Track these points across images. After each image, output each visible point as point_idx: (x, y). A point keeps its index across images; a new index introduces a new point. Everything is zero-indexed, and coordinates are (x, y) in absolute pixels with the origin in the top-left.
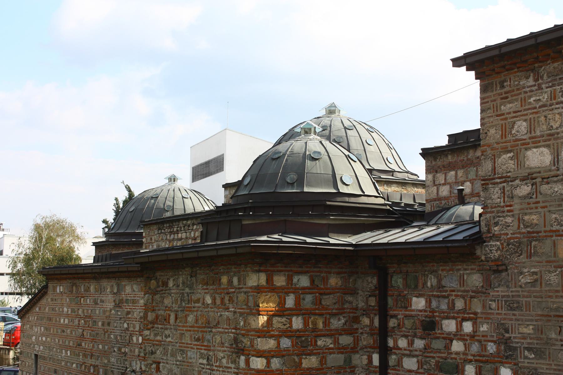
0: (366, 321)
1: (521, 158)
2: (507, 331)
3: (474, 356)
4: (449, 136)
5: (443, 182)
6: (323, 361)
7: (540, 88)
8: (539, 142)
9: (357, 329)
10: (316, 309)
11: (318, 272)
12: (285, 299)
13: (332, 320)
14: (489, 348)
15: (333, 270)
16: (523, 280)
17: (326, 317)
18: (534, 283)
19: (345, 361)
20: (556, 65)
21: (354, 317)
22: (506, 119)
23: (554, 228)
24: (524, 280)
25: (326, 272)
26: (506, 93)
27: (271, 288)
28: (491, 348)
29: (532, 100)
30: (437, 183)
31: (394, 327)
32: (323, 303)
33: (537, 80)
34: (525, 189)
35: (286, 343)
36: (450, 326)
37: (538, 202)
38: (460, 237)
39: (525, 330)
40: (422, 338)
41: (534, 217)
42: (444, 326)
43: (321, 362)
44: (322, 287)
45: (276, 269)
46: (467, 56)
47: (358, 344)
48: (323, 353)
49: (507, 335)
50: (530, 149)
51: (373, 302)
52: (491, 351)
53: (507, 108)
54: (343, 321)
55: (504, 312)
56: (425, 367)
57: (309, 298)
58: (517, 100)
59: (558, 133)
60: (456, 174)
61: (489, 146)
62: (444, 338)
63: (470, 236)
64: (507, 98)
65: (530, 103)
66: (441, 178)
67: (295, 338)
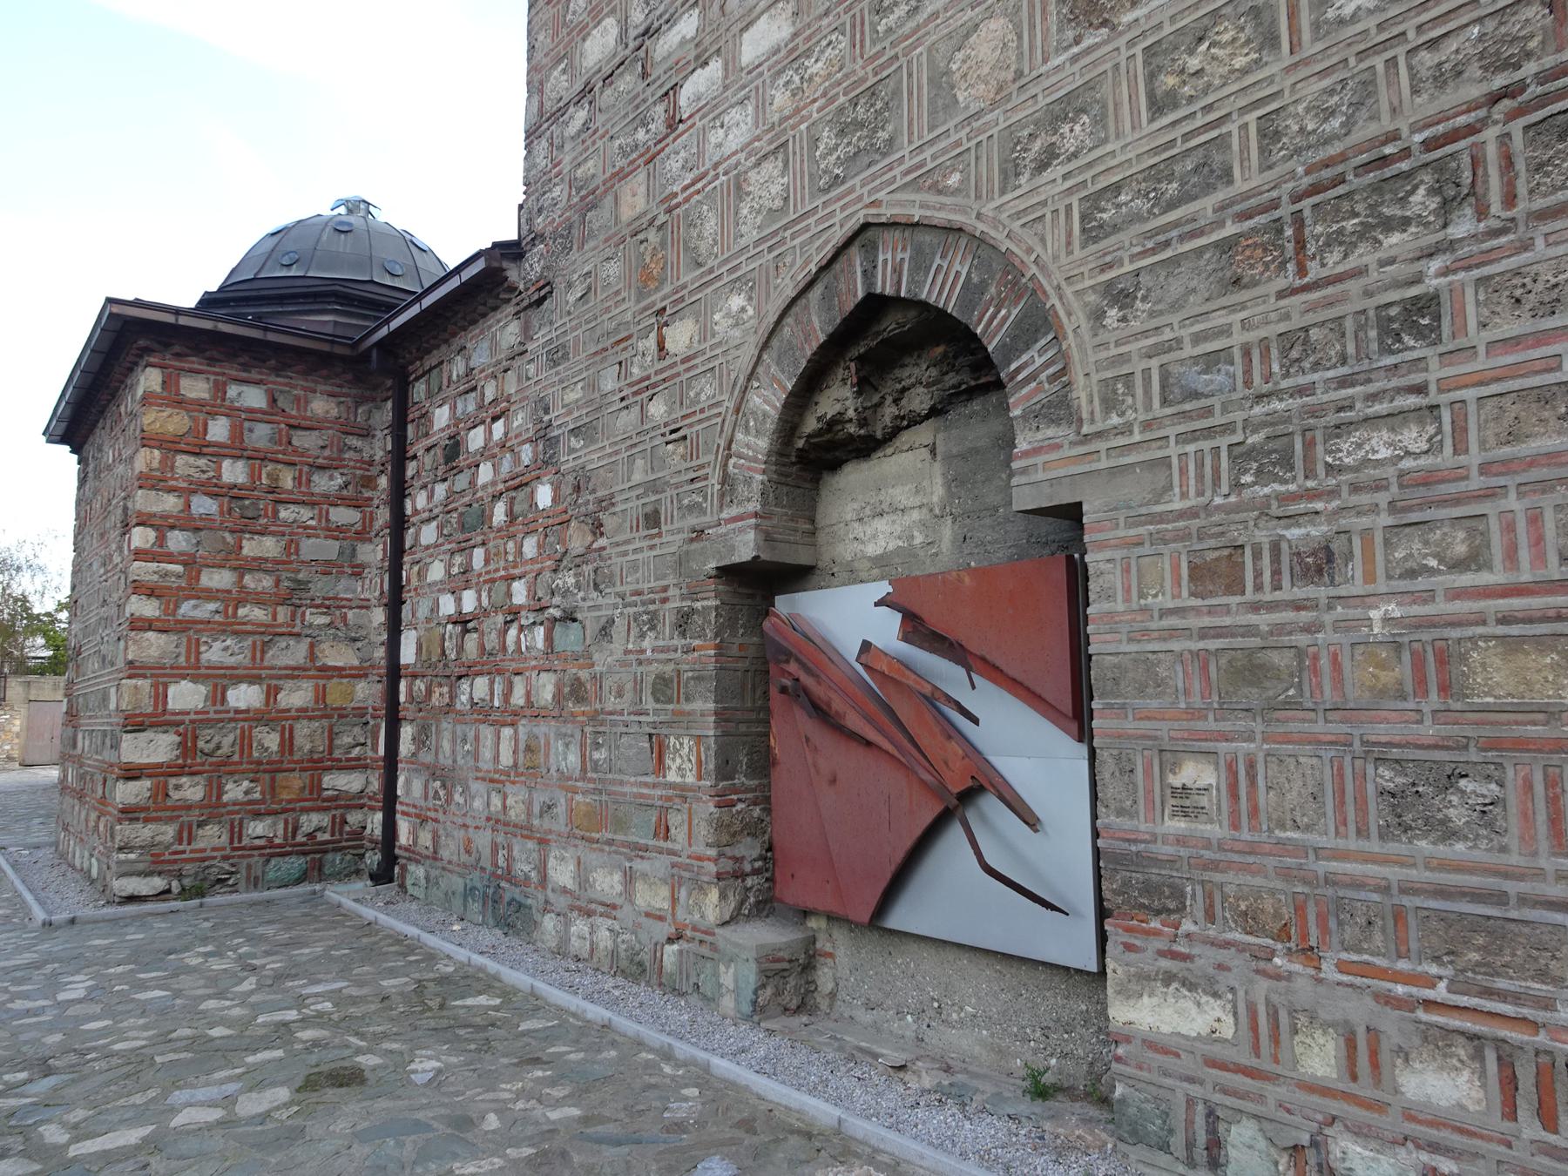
6: (292, 547)
9: (371, 499)
10: (278, 452)
11: (286, 385)
12: (206, 425)
13: (315, 478)
15: (320, 387)
17: (301, 471)
19: (340, 554)
21: (363, 477)
25: (304, 389)
32: (295, 442)
35: (204, 505)
43: (287, 548)
44: (294, 413)
45: (186, 366)
47: (371, 526)
54: (340, 481)
67: (226, 500)
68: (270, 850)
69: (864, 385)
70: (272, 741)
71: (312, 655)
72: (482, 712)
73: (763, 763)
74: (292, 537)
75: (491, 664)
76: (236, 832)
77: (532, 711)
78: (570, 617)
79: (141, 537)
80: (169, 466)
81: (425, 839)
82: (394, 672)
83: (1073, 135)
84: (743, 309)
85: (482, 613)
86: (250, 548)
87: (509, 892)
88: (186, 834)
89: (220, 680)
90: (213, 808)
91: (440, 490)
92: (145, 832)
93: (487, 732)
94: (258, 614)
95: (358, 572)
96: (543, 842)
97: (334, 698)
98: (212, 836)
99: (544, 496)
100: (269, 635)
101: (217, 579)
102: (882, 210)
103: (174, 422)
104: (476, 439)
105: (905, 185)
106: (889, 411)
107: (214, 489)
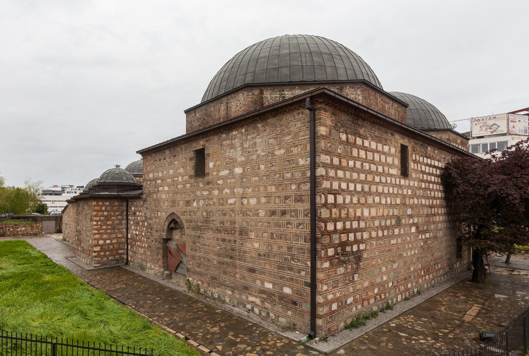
6: (113, 222)
24: (149, 203)
27: (98, 205)
34: (149, 183)
35: (102, 218)
48: (113, 221)
53: (147, 164)
57: (109, 208)
68: (112, 260)
69: (175, 224)
70: (112, 247)
71: (116, 236)
72: (139, 246)
73: (167, 257)
74: (113, 221)
75: (140, 241)
76: (108, 258)
77: (144, 247)
78: (149, 238)
79: (95, 223)
80: (98, 213)
81: (132, 259)
82: (127, 238)
83: (186, 214)
85: (139, 235)
86: (108, 223)
87: (143, 267)
88: (102, 259)
89: (105, 240)
90: (105, 256)
92: (97, 259)
93: (140, 249)
94: (109, 231)
95: (122, 224)
96: (146, 262)
97: (119, 240)
98: (105, 259)
99: (146, 224)
100: (111, 234)
101: (104, 227)
103: (98, 208)
104: (138, 213)
106: (177, 227)
107: (103, 216)
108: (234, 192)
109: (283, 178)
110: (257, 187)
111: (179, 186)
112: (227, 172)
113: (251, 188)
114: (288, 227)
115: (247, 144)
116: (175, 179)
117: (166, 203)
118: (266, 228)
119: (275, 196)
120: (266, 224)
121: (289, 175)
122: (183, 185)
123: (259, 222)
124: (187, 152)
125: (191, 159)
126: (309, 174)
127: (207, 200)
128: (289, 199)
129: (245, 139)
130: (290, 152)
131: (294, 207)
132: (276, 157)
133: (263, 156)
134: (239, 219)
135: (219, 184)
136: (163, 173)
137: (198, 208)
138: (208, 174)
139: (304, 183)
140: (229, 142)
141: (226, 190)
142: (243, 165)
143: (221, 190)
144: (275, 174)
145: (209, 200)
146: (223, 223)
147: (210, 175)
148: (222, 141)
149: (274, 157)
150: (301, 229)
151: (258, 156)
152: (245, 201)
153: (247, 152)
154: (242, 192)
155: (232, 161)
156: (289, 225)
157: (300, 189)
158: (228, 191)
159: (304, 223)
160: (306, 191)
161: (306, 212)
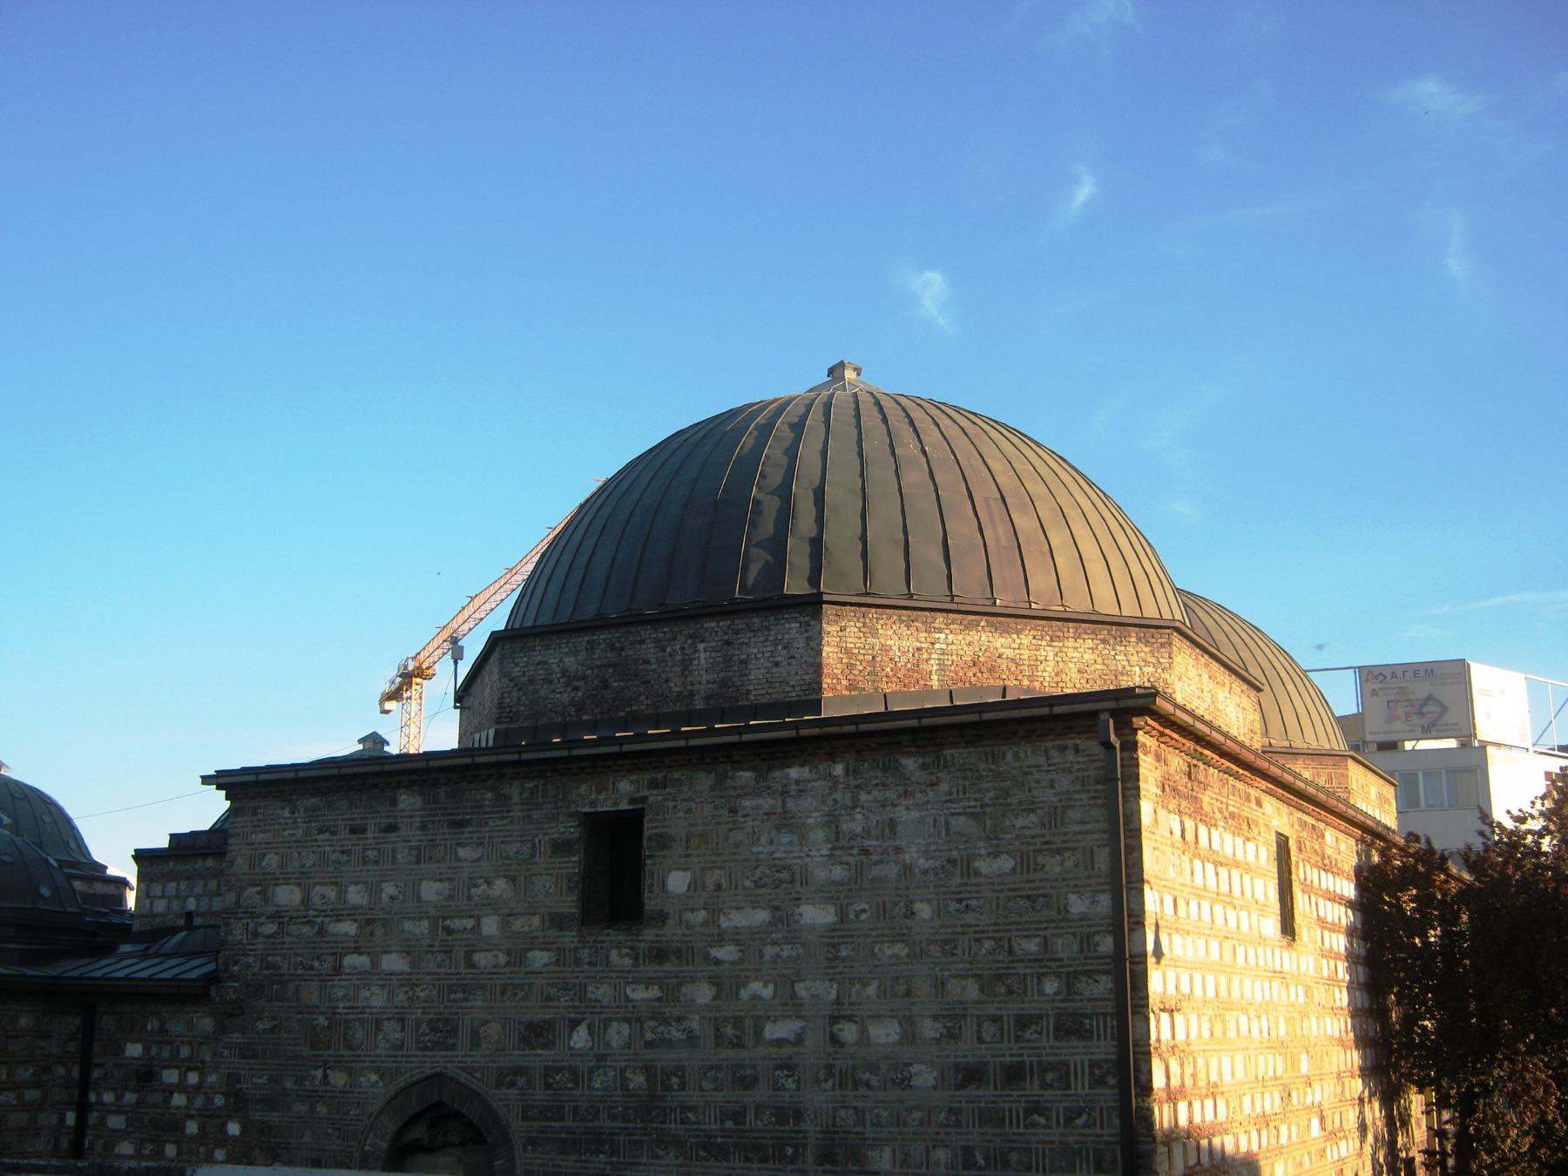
0: (61, 1071)
1: (269, 894)
2: (238, 1081)
3: (198, 1110)
4: (172, 836)
5: (160, 894)
7: (295, 822)
8: (290, 878)
14: (216, 1101)
16: (261, 1026)
18: (272, 1030)
20: (314, 800)
22: (256, 849)
23: (299, 972)
26: (258, 821)
28: (219, 1100)
29: (286, 833)
30: (151, 894)
31: (98, 1079)
33: (293, 813)
36: (171, 1076)
37: (284, 943)
38: (193, 975)
39: (260, 1081)
40: (134, 1091)
41: (279, 959)
42: (164, 1077)
46: (220, 774)
49: (238, 1086)
50: (280, 885)
51: (72, 1047)
52: (219, 1104)
54: (32, 1071)
55: (237, 1061)
56: (136, 1124)
58: (270, 831)
59: (310, 872)
60: (178, 885)
61: (235, 875)
62: (164, 1091)
63: (206, 974)
64: (259, 826)
65: (283, 837)
66: (157, 889)
83: (521, 1081)
84: (377, 1082)
91: (130, 1098)
99: (234, 1129)
102: (448, 1072)
104: (171, 1076)
105: (458, 1067)
108: (794, 995)
109: (1011, 952)
110: (902, 981)
111: (481, 958)
112: (761, 916)
113: (874, 985)
114: (1034, 1125)
115: (854, 820)
116: (457, 924)
117: (392, 1031)
118: (943, 1130)
119: (978, 1017)
120: (943, 1115)
121: (1032, 946)
122: (509, 953)
123: (909, 1110)
124: (536, 814)
125: (561, 847)
126: (1106, 945)
127: (653, 1023)
128: (1034, 1027)
129: (849, 803)
130: (1035, 870)
131: (1055, 1054)
132: (982, 880)
133: (925, 872)
134: (817, 1099)
135: (717, 962)
136: (374, 890)
137: (601, 1058)
138: (662, 917)
139: (1089, 974)
140: (771, 802)
141: (755, 986)
142: (836, 894)
143: (727, 986)
144: (978, 940)
145: (666, 1022)
146: (738, 1116)
147: (671, 922)
148: (737, 797)
149: (974, 880)
150: (1084, 1126)
151: (907, 869)
152: (848, 1032)
153: (855, 851)
154: (833, 996)
155: (784, 875)
156: (1036, 1117)
157: (1075, 993)
158: (767, 992)
159: (1092, 1109)
160: (1097, 1000)
161: (1097, 1072)
